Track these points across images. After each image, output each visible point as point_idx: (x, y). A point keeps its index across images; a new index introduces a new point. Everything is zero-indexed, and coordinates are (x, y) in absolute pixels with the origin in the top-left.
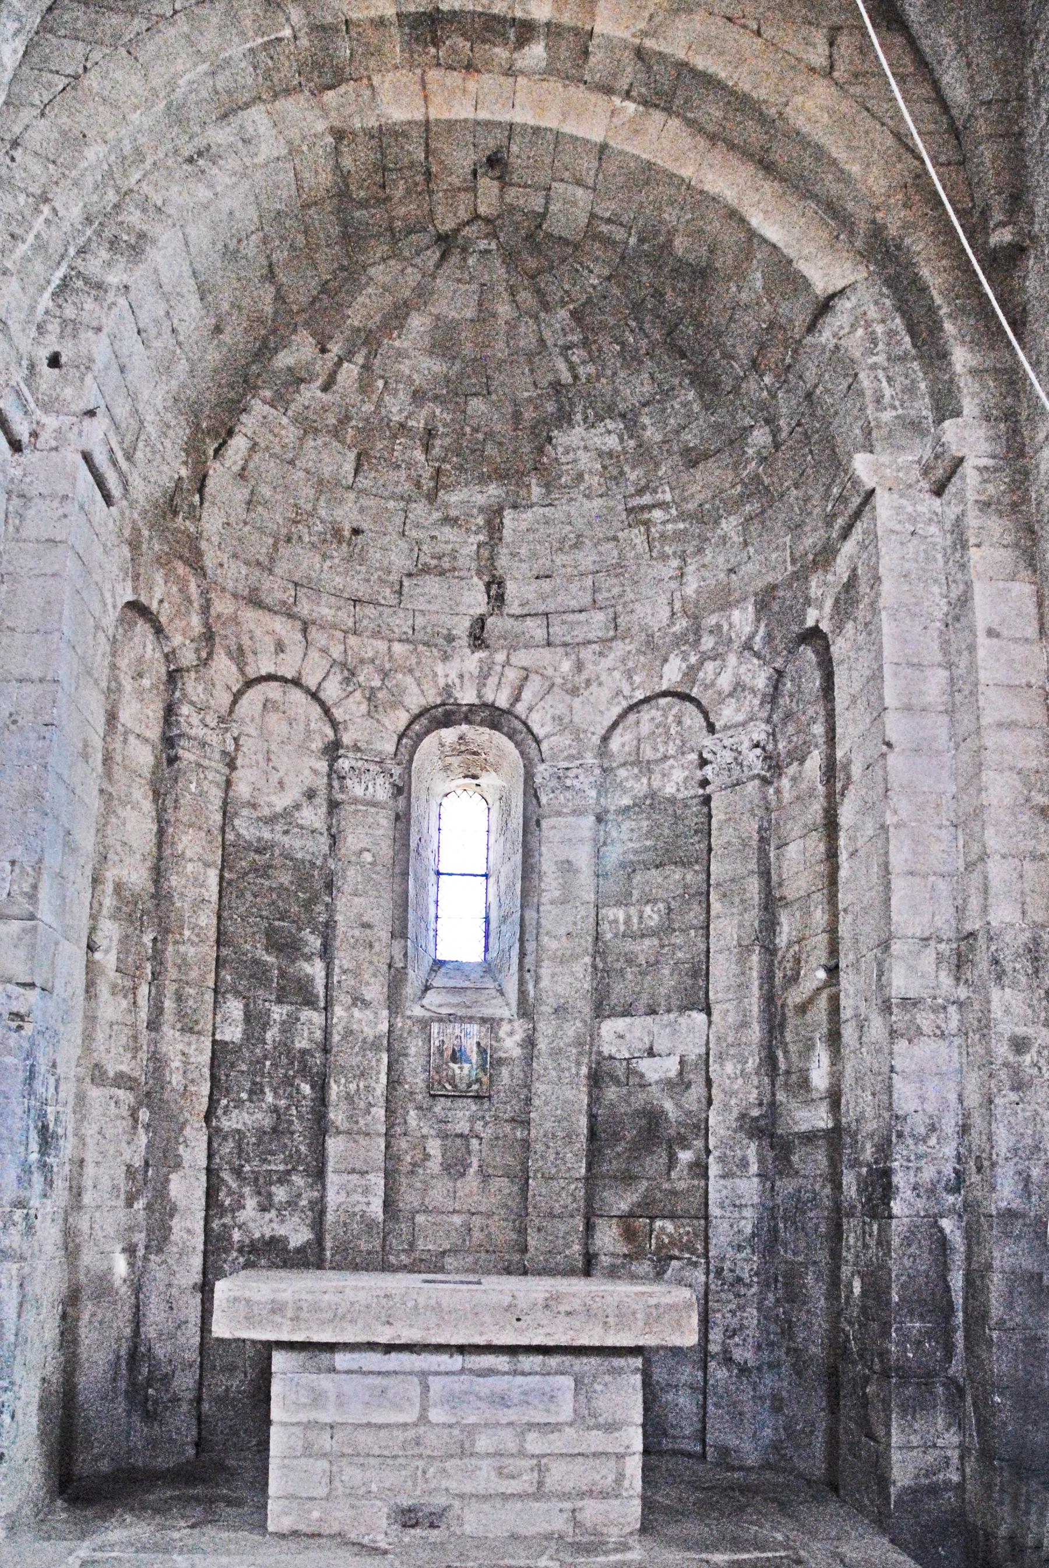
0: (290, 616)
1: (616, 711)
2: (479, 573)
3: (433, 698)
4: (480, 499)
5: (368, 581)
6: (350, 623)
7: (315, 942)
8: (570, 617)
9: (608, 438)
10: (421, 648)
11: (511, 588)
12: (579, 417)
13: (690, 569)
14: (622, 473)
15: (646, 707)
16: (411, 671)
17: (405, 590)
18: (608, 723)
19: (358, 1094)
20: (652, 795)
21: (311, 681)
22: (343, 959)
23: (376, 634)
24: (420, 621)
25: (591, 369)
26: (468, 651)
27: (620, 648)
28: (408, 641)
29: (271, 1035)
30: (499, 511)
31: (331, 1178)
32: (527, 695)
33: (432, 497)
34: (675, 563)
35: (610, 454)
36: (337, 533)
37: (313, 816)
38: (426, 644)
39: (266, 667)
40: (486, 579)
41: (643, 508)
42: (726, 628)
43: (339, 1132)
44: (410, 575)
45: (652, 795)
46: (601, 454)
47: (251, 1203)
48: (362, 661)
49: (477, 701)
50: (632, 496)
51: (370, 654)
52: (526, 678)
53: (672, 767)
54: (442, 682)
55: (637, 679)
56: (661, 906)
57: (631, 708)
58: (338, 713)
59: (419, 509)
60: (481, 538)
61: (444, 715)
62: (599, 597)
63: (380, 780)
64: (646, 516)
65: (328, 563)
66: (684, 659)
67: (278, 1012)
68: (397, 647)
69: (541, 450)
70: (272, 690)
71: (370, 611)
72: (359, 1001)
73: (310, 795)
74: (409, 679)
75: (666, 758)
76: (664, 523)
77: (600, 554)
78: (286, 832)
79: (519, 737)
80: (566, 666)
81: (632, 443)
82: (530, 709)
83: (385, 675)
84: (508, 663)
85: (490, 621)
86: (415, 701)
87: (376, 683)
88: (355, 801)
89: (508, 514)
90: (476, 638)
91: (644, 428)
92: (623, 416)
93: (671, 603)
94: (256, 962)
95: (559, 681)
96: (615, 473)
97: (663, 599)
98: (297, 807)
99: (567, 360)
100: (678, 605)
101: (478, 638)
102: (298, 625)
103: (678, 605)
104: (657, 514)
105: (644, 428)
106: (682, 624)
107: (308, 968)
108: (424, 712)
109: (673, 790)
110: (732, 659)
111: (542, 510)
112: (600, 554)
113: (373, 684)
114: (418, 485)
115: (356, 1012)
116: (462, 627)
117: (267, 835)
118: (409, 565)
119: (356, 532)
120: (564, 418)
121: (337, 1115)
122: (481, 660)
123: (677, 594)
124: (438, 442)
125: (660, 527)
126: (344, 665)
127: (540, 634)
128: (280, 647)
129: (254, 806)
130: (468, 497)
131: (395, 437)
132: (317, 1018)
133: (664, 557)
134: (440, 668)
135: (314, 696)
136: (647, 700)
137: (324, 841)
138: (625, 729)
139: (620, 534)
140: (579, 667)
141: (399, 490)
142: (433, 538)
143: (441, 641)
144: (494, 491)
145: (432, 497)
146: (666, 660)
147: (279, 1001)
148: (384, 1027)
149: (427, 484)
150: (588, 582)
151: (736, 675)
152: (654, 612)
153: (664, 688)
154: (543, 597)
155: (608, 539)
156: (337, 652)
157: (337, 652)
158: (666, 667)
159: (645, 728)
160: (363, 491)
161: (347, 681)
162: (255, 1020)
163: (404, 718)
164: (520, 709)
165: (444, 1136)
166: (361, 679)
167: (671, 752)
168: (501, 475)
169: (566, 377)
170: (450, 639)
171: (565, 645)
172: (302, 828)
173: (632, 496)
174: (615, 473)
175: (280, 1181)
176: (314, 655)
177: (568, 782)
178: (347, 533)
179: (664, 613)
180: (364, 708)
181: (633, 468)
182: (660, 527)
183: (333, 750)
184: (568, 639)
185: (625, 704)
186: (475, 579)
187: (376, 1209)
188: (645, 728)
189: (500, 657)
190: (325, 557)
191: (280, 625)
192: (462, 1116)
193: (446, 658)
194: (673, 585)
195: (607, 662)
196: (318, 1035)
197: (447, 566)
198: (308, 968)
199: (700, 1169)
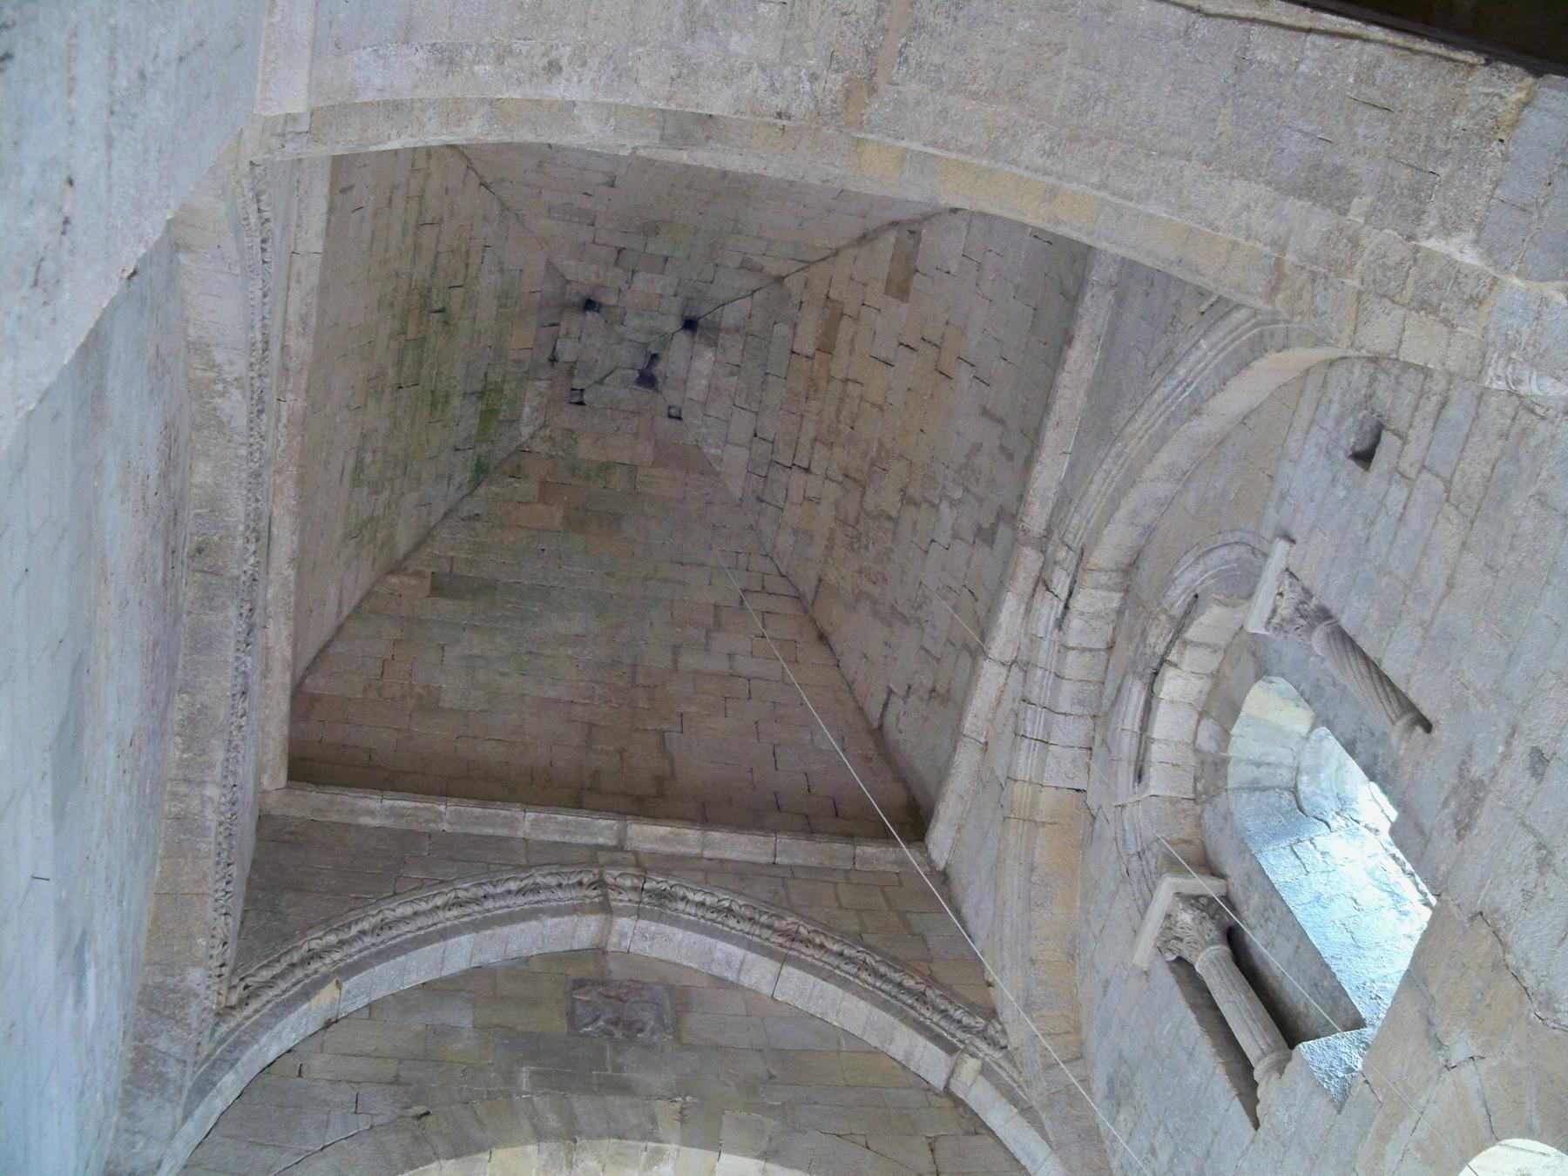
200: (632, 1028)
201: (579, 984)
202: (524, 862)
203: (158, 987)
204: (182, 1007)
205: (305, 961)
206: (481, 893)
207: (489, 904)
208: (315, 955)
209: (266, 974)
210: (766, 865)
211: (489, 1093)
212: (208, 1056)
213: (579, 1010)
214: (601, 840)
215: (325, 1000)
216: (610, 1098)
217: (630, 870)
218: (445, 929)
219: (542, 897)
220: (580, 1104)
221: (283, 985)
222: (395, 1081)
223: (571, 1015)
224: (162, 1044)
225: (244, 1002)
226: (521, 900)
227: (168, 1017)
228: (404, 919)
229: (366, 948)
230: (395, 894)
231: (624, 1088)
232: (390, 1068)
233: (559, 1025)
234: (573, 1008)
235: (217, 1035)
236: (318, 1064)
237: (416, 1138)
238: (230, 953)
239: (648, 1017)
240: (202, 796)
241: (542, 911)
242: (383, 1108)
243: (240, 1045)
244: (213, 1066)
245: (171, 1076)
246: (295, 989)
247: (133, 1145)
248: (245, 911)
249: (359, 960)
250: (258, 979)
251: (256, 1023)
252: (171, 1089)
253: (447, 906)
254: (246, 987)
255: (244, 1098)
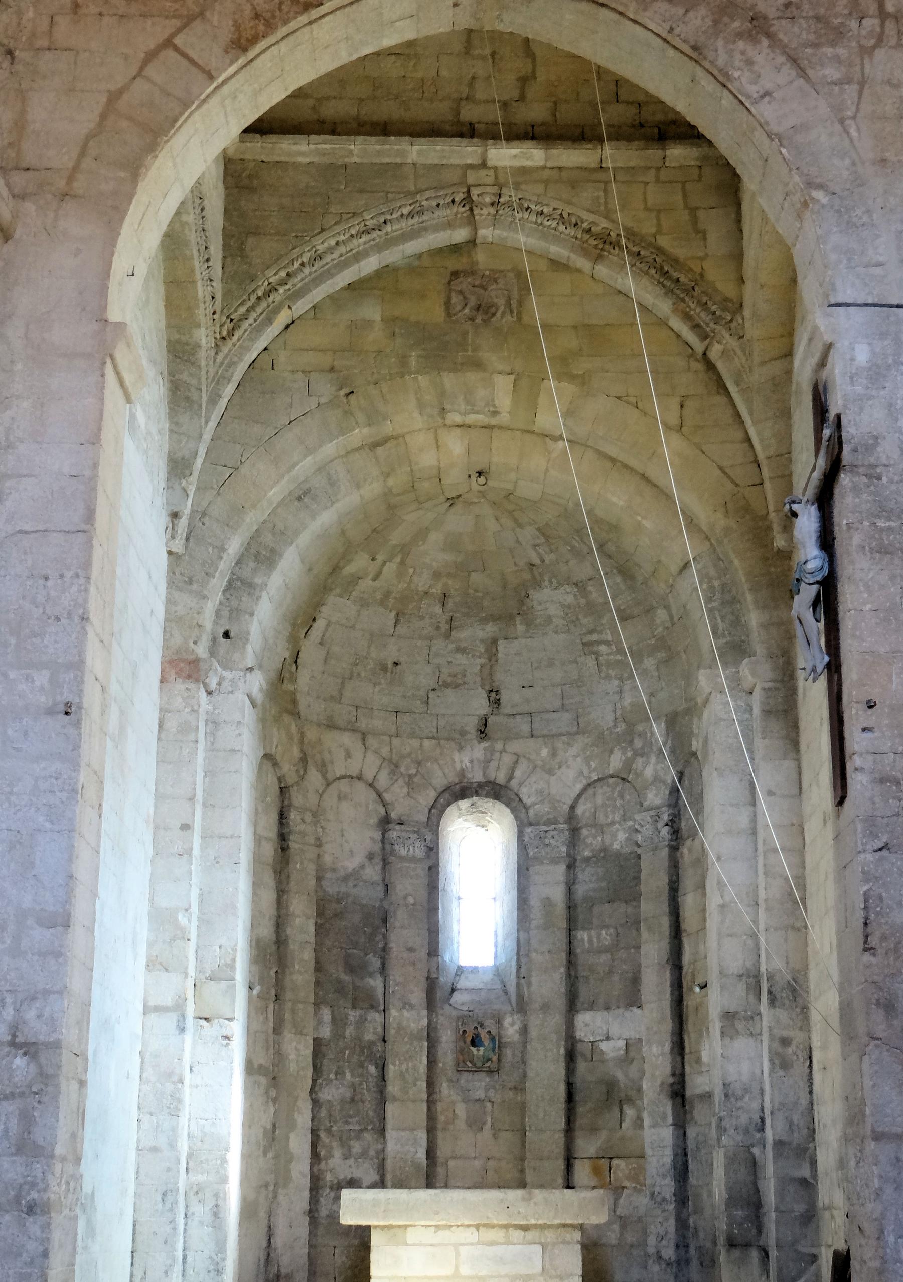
0: (354, 730)
1: (579, 787)
2: (483, 686)
3: (453, 778)
4: (481, 634)
5: (404, 697)
6: (393, 731)
7: (376, 963)
8: (546, 716)
9: (567, 595)
10: (442, 742)
11: (505, 697)
12: (547, 583)
13: (626, 688)
14: (578, 619)
15: (599, 785)
16: (436, 760)
17: (430, 700)
18: (573, 795)
19: (407, 1069)
20: (604, 849)
21: (369, 775)
22: (396, 974)
23: (413, 735)
24: (442, 723)
25: (553, 556)
26: (475, 742)
27: (581, 741)
28: (433, 738)
29: (349, 1031)
30: (495, 641)
31: (391, 1134)
32: (518, 773)
33: (448, 636)
34: (616, 682)
35: (569, 607)
36: (384, 668)
37: (372, 873)
38: (448, 740)
39: (339, 771)
40: (488, 688)
41: (591, 644)
42: (649, 735)
43: (395, 1099)
44: (434, 690)
45: (604, 849)
46: (563, 606)
47: (337, 1153)
48: (403, 757)
49: (483, 780)
50: (585, 634)
51: (408, 750)
52: (516, 762)
53: (618, 830)
54: (458, 766)
55: (593, 765)
56: (612, 930)
57: (589, 785)
58: (387, 797)
59: (439, 644)
60: (483, 660)
61: (461, 791)
62: (567, 702)
63: (418, 844)
64: (595, 648)
65: (377, 688)
66: (624, 754)
67: (353, 1015)
68: (427, 743)
69: (522, 603)
70: (343, 786)
71: (407, 718)
72: (407, 1005)
73: (370, 857)
74: (436, 767)
75: (613, 823)
76: (607, 654)
77: (566, 671)
78: (355, 886)
79: (514, 804)
80: (545, 752)
81: (583, 601)
82: (520, 785)
83: (419, 763)
84: (504, 751)
85: (489, 721)
86: (440, 780)
87: (413, 771)
88: (402, 858)
89: (502, 645)
90: (482, 732)
91: (591, 593)
92: (576, 584)
93: (615, 711)
94: (339, 981)
95: (539, 763)
96: (574, 618)
97: (610, 708)
98: (362, 867)
99: (536, 551)
100: (619, 713)
101: (483, 731)
102: (359, 736)
103: (619, 713)
104: (603, 648)
105: (591, 593)
106: (621, 727)
107: (372, 982)
108: (447, 789)
109: (618, 847)
110: (653, 759)
111: (524, 641)
112: (566, 671)
113: (411, 772)
114: (438, 628)
115: (406, 1013)
116: (472, 724)
117: (343, 889)
118: (432, 683)
119: (396, 664)
120: (537, 584)
121: (393, 1088)
122: (485, 749)
123: (618, 706)
124: (450, 600)
125: (605, 657)
126: (390, 761)
127: (526, 728)
128: (348, 755)
129: (334, 870)
130: (474, 633)
131: (421, 600)
132: (378, 1017)
133: (608, 677)
134: (456, 757)
135: (371, 785)
136: (599, 780)
137: (380, 888)
138: (586, 799)
139: (579, 659)
140: (554, 754)
141: (425, 632)
142: (449, 662)
143: (457, 736)
144: (491, 629)
145: (448, 636)
146: (611, 752)
147: (354, 1007)
148: (425, 1022)
149: (444, 627)
150: (559, 691)
151: (655, 770)
152: (603, 715)
153: (611, 772)
154: (528, 701)
155: (570, 662)
156: (385, 751)
157: (385, 751)
158: (612, 756)
159: (600, 800)
160: (400, 637)
161: (392, 773)
162: (338, 1022)
163: (433, 795)
164: (514, 784)
165: (466, 1101)
166: (403, 769)
167: (617, 819)
168: (494, 618)
169: (537, 561)
170: (463, 733)
171: (544, 736)
172: (365, 881)
173: (585, 634)
174: (574, 618)
175: (358, 1138)
176: (371, 757)
177: (547, 841)
178: (390, 665)
179: (610, 717)
180: (405, 790)
181: (585, 617)
182: (605, 657)
183: (385, 822)
184: (545, 732)
185: (585, 782)
186: (480, 688)
187: (421, 1155)
188: (600, 800)
189: (499, 746)
190: (375, 684)
191: (347, 739)
192: (479, 1085)
193: (461, 748)
194: (616, 697)
195: (573, 751)
196: (380, 1029)
197: (460, 681)
198: (372, 982)
199: (639, 1123)
200: (485, 310)
201: (455, 274)
202: (412, 188)
203: (178, 341)
204: (193, 354)
205: (267, 294)
206: (382, 220)
207: (389, 228)
208: (272, 290)
209: (243, 310)
210: (594, 170)
211: (391, 374)
212: (214, 377)
213: (455, 299)
214: (469, 161)
215: (284, 317)
216: (468, 374)
217: (488, 189)
218: (358, 253)
219: (425, 217)
220: (449, 380)
221: (253, 315)
222: (332, 369)
223: (448, 304)
224: (185, 377)
225: (231, 333)
226: (411, 222)
227: (186, 361)
228: (330, 250)
229: (306, 277)
230: (323, 230)
231: (477, 365)
232: (326, 360)
233: (438, 314)
234: (449, 298)
235: (218, 360)
236: (282, 357)
237: (346, 412)
238: (218, 306)
239: (501, 303)
240: (181, 221)
241: (426, 229)
242: (325, 389)
243: (232, 364)
244: (218, 383)
245: (194, 398)
246: (262, 317)
247: (180, 442)
248: (224, 257)
249: (301, 288)
250: (239, 313)
251: (240, 347)
252: (196, 406)
253: (360, 234)
254: (232, 320)
255: (241, 388)
